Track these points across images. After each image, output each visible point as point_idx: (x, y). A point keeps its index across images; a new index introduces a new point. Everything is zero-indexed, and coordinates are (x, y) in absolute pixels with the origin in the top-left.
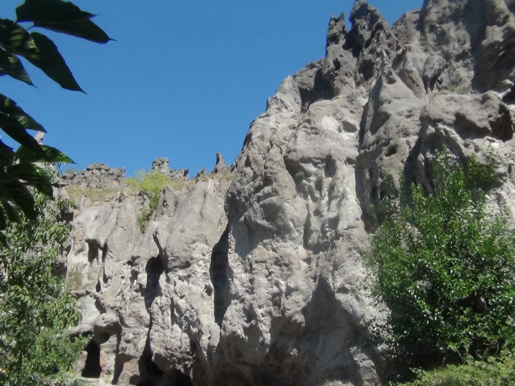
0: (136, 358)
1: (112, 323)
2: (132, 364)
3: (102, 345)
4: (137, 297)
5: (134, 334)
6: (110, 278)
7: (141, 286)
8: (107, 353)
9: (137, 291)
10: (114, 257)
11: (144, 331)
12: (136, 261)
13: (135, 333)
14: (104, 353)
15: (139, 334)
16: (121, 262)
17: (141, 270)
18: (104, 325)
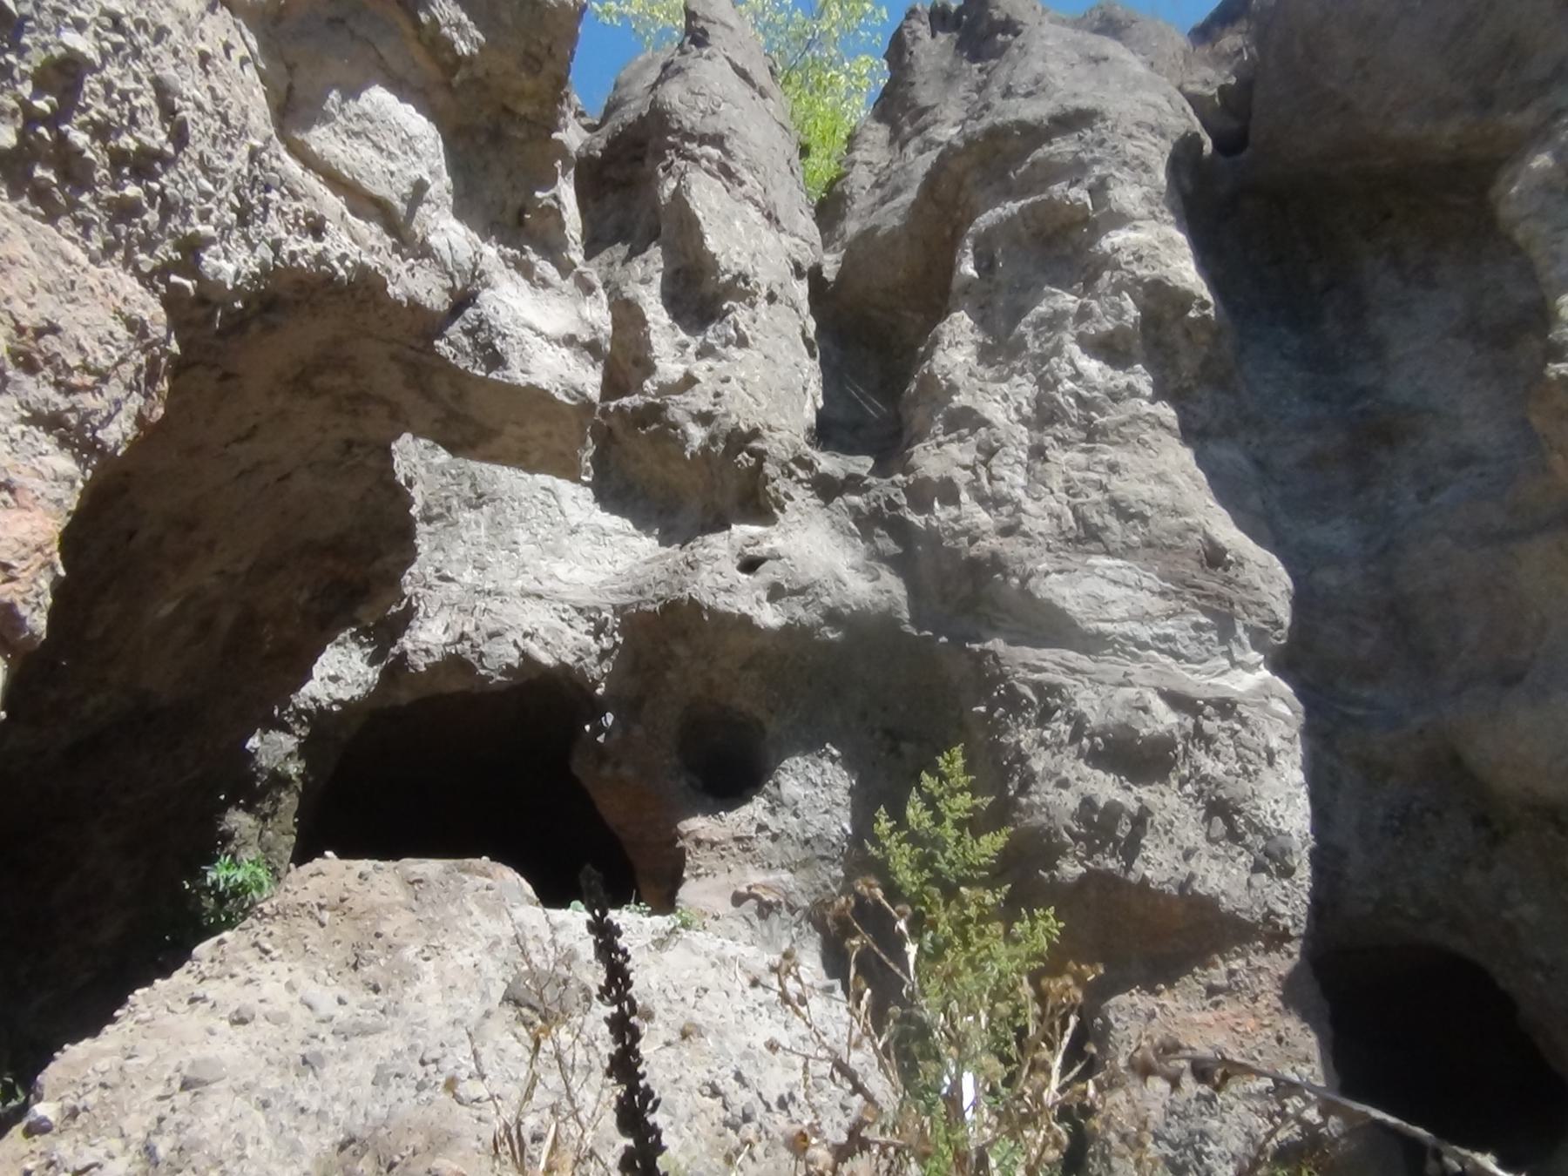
0: (1276, 938)
1: (832, 616)
2: (1229, 1009)
3: (698, 824)
4: (1114, 396)
5: (1177, 701)
6: (740, 288)
7: (1161, 300)
8: (765, 910)
9: (1110, 349)
10: (746, 176)
11: (1265, 692)
12: (1039, 153)
13: (1192, 691)
14: (724, 906)
15: (1226, 707)
16: (786, 240)
17: (1127, 195)
18: (769, 617)
